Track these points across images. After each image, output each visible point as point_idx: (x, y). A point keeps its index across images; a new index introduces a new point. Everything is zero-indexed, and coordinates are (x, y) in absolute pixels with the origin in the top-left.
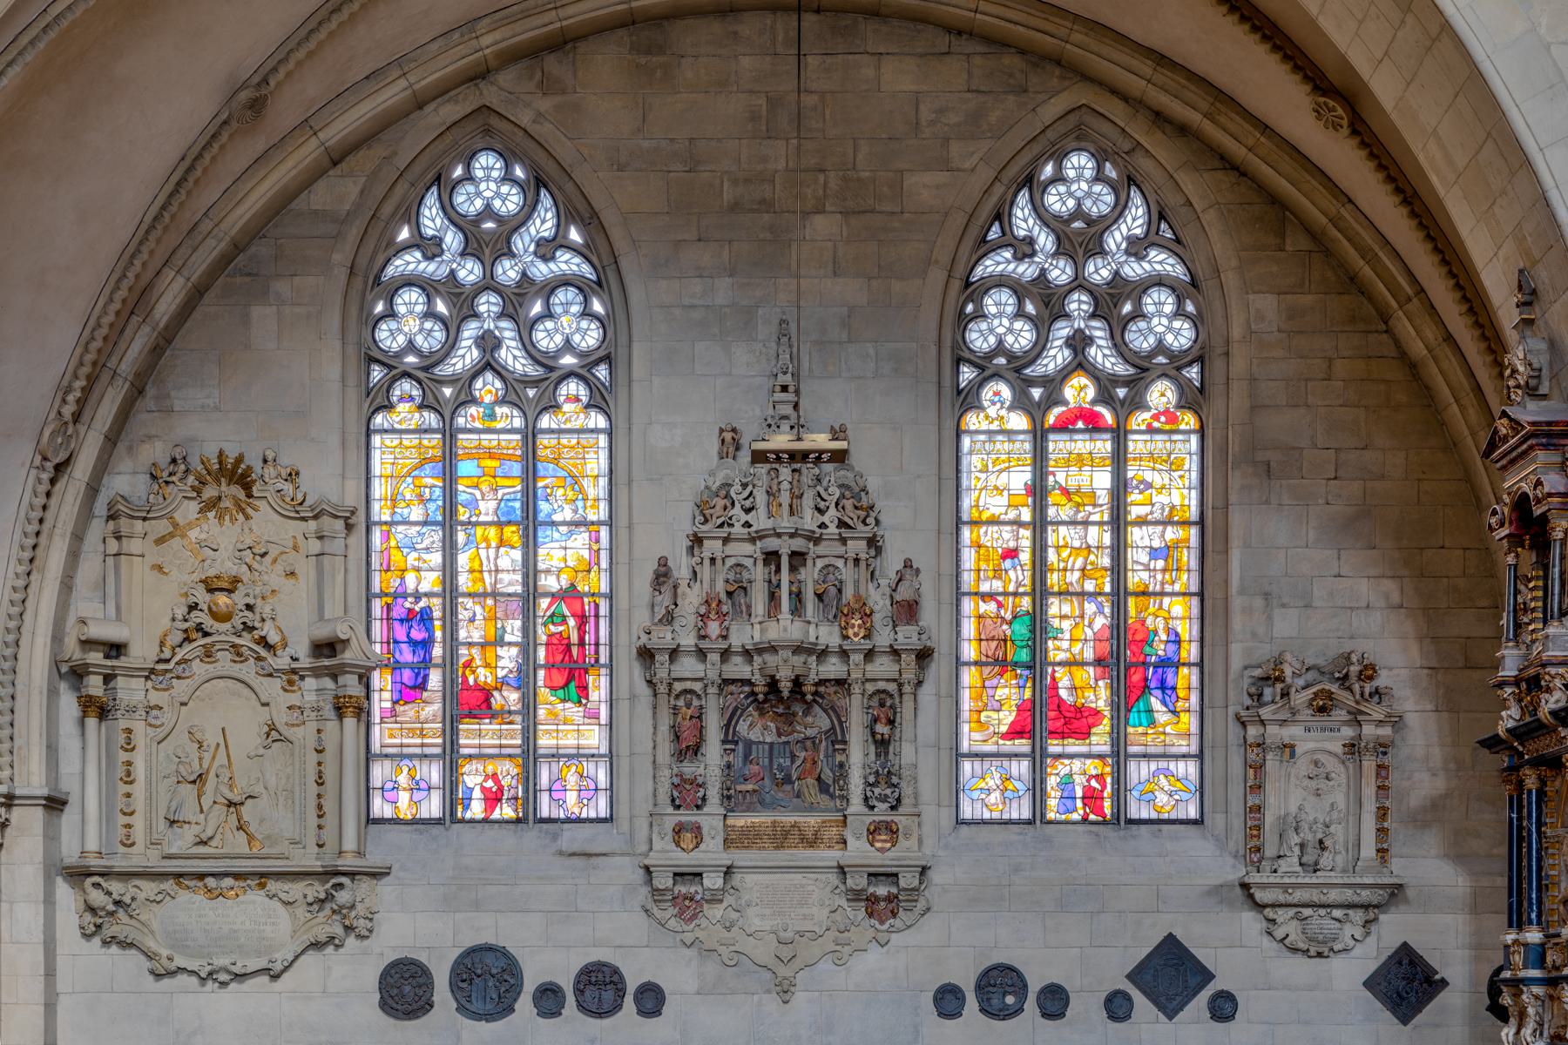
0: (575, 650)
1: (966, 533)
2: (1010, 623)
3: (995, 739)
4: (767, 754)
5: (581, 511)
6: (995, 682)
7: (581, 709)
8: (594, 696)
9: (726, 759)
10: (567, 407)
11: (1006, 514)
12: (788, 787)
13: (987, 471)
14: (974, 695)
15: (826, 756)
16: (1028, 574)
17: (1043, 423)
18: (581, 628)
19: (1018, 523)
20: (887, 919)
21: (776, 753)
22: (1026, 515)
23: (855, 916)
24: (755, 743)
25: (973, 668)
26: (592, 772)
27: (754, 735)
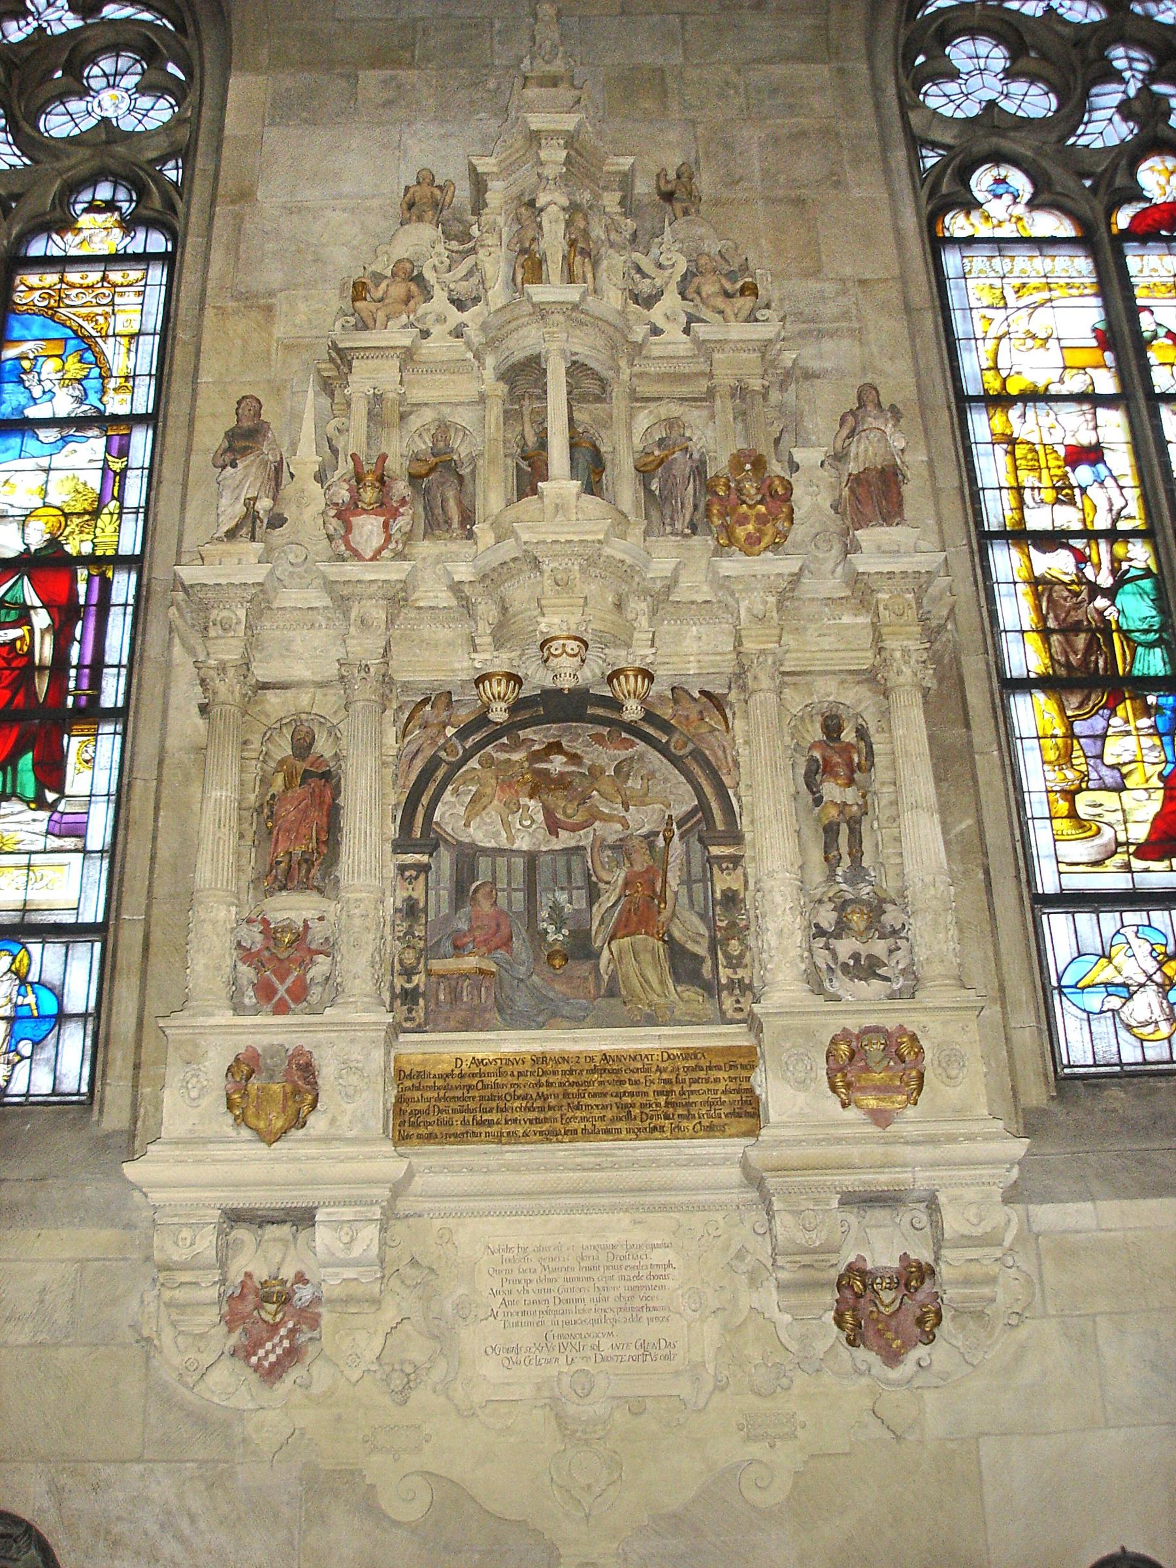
0: (42, 685)
1: (980, 424)
2: (1111, 594)
3: (1119, 859)
4: (519, 880)
5: (93, 399)
6: (1098, 723)
7: (44, 815)
8: (77, 781)
9: (402, 894)
10: (85, 221)
11: (1061, 381)
12: (582, 969)
13: (1006, 307)
14: (1051, 755)
15: (688, 881)
16: (1133, 494)
17: (1109, 225)
18: (62, 637)
19: (1091, 399)
20: (908, 1345)
21: (543, 876)
22: (1106, 383)
23: (804, 1340)
24: (484, 851)
25: (1040, 697)
26: (52, 974)
27: (480, 834)
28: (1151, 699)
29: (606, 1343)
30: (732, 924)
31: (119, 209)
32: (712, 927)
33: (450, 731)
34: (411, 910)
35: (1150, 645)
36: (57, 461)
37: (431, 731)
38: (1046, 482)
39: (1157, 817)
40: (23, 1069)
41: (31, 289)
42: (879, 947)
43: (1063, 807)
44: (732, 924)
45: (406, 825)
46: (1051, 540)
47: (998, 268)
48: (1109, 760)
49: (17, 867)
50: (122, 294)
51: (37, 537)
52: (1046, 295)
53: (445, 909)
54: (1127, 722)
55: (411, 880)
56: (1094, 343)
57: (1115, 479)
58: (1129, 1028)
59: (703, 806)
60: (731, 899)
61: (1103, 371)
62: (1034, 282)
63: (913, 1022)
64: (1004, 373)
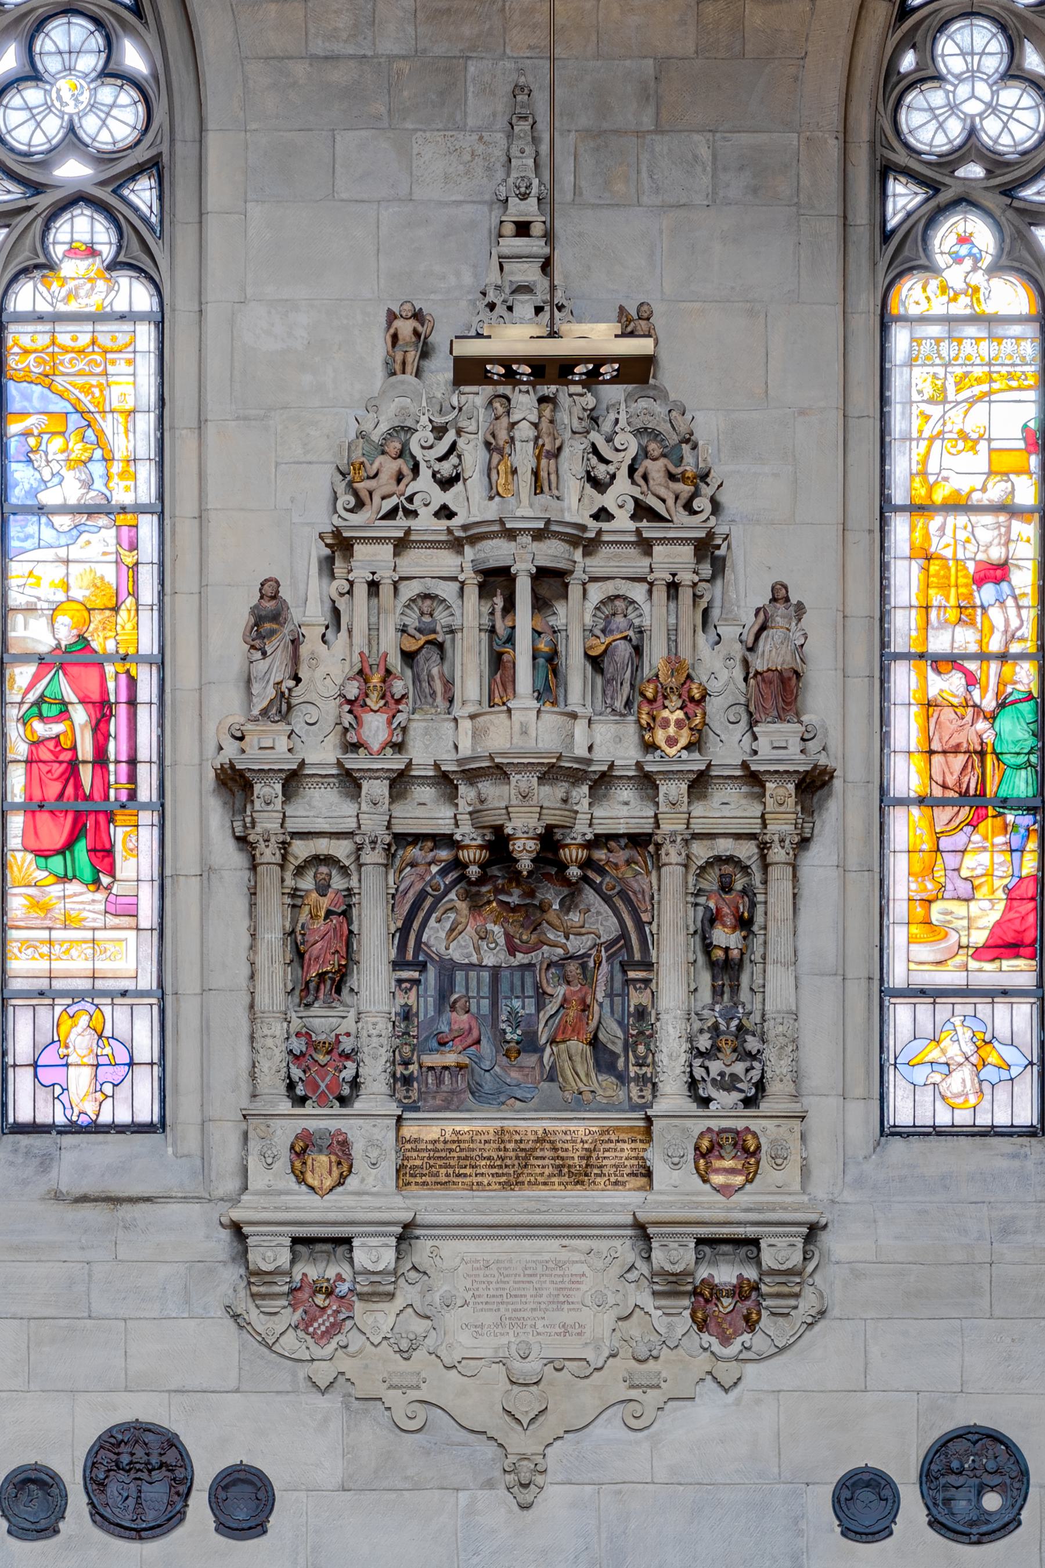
2: (992, 717)
3: (960, 959)
4: (485, 991)
5: (99, 484)
7: (100, 896)
8: (125, 867)
9: (401, 1000)
10: (70, 268)
11: (984, 489)
12: (529, 1060)
13: (945, 401)
14: (917, 868)
15: (610, 995)
19: (1008, 509)
21: (504, 987)
25: (915, 811)
26: (122, 1029)
28: (1010, 818)
29: (539, 1324)
30: (641, 1033)
31: (98, 254)
32: (626, 1032)
33: (434, 869)
34: (407, 1015)
35: (1019, 767)
36: (75, 553)
37: (420, 869)
38: (953, 602)
39: (998, 924)
40: (108, 1104)
41: (26, 352)
42: (739, 1068)
43: (920, 911)
44: (641, 1033)
45: (402, 947)
46: (951, 661)
47: (944, 353)
48: (965, 873)
49: (85, 941)
50: (113, 362)
51: (66, 635)
52: (985, 388)
53: (431, 1013)
54: (986, 838)
55: (407, 991)
56: (1021, 445)
57: (1015, 598)
58: (943, 1098)
59: (624, 935)
60: (641, 1013)
61: (1025, 478)
62: (978, 371)
63: (754, 1125)
64: (932, 479)
